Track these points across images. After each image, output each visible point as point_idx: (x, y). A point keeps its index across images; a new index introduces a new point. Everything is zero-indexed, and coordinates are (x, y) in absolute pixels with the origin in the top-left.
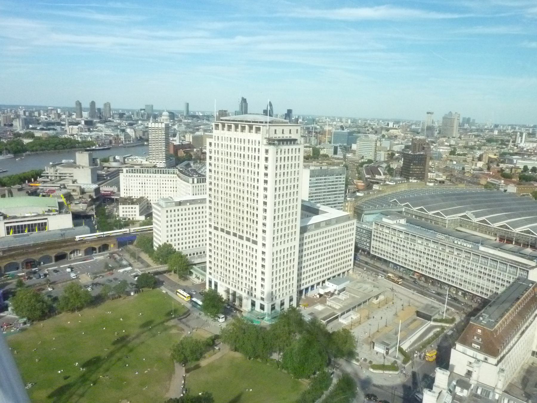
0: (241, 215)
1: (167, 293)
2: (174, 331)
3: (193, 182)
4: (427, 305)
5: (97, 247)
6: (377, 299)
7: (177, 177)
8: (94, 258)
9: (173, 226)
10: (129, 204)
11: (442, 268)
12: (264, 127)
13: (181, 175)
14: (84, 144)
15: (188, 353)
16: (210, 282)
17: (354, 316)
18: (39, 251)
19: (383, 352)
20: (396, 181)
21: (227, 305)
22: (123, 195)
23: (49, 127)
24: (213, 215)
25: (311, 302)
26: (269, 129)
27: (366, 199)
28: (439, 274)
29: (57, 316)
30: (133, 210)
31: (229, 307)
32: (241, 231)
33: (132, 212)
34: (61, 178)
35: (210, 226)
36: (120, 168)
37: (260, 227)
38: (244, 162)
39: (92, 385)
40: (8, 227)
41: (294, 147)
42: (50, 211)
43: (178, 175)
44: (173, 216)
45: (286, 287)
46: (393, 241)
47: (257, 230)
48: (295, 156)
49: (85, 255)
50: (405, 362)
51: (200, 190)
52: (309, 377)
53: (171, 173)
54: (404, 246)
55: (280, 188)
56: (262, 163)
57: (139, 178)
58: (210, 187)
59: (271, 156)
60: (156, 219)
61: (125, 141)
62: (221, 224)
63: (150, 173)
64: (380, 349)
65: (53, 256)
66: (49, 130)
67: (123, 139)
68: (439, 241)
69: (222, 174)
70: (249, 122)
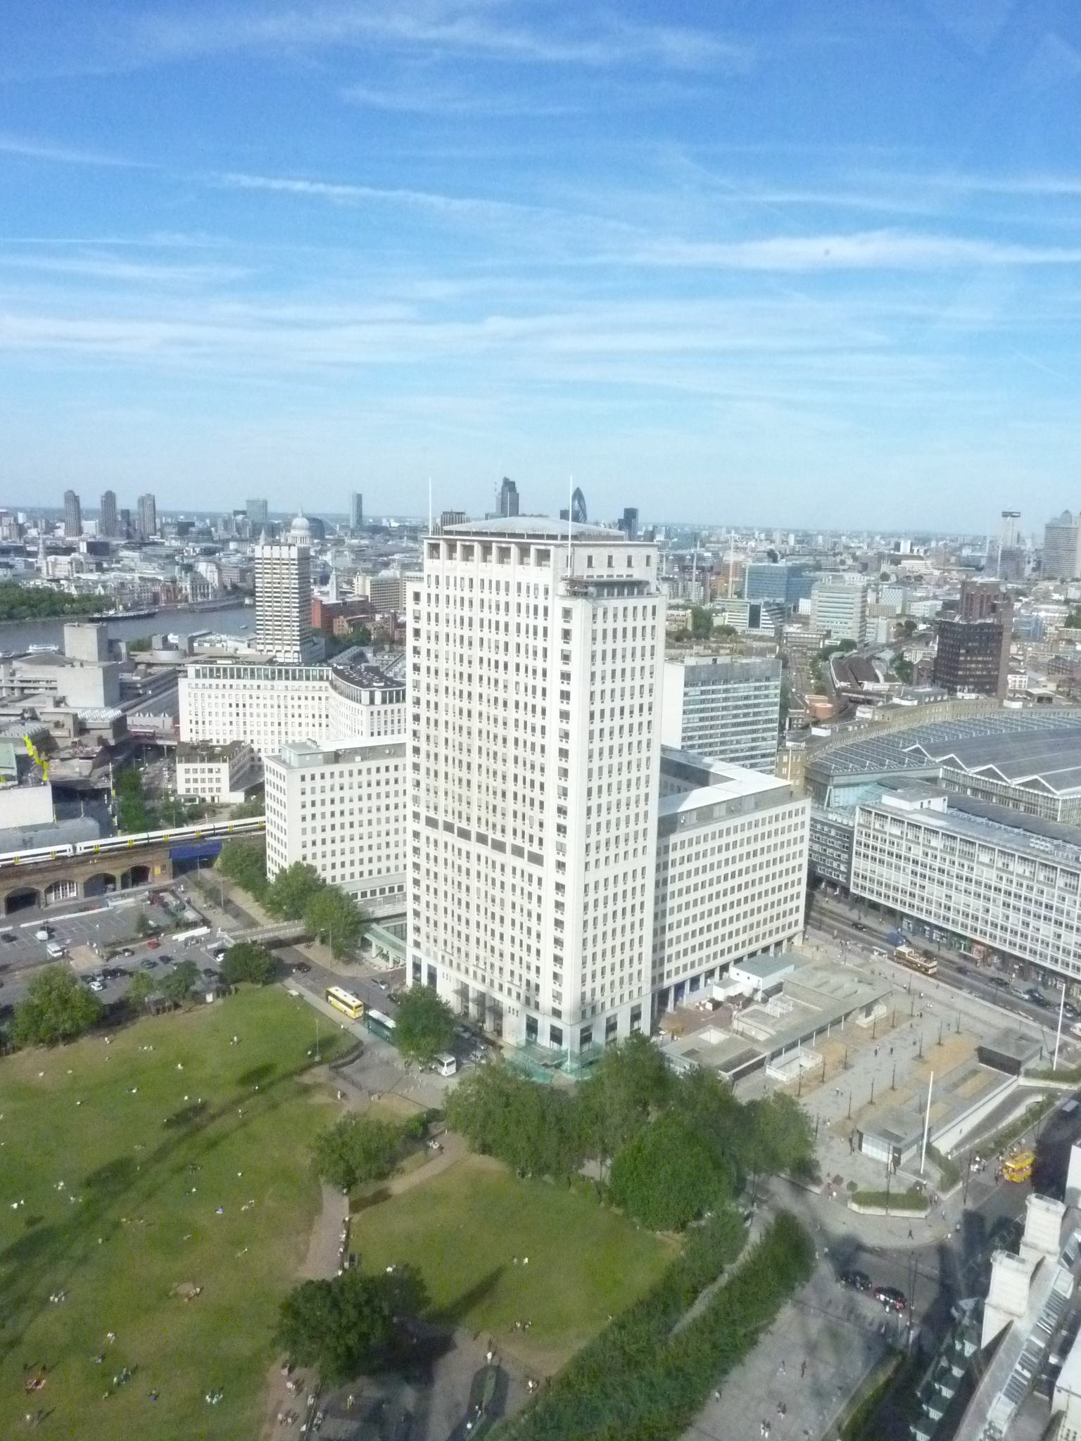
0: (498, 784)
1: (301, 996)
2: (319, 1099)
3: (372, 702)
4: (1008, 1032)
5: (117, 874)
6: (868, 1015)
8: (110, 903)
9: (318, 817)
10: (202, 760)
11: (1047, 930)
12: (560, 549)
13: (340, 682)
14: (88, 605)
15: (356, 1157)
16: (417, 968)
17: (806, 1060)
19: (885, 1160)
20: (919, 697)
21: (461, 1029)
22: (185, 737)
24: (423, 786)
25: (691, 1022)
26: (573, 553)
27: (839, 746)
28: (1039, 948)
29: (12, 1057)
30: (214, 775)
31: (466, 1035)
32: (499, 828)
33: (211, 780)
34: (25, 690)
35: (416, 816)
36: (180, 665)
37: (551, 819)
38: (506, 644)
39: (100, 1241)
41: (639, 602)
43: (331, 683)
44: (318, 790)
45: (622, 979)
46: (911, 856)
47: (541, 825)
48: (644, 628)
50: (946, 1185)
51: (389, 722)
52: (682, 1226)
53: (314, 679)
54: (941, 871)
55: (602, 712)
56: (555, 644)
58: (416, 711)
59: (578, 625)
60: (273, 798)
61: (195, 595)
62: (446, 811)
63: (259, 677)
64: (876, 1151)
67: (189, 591)
68: (1036, 856)
69: (447, 675)
70: (521, 536)
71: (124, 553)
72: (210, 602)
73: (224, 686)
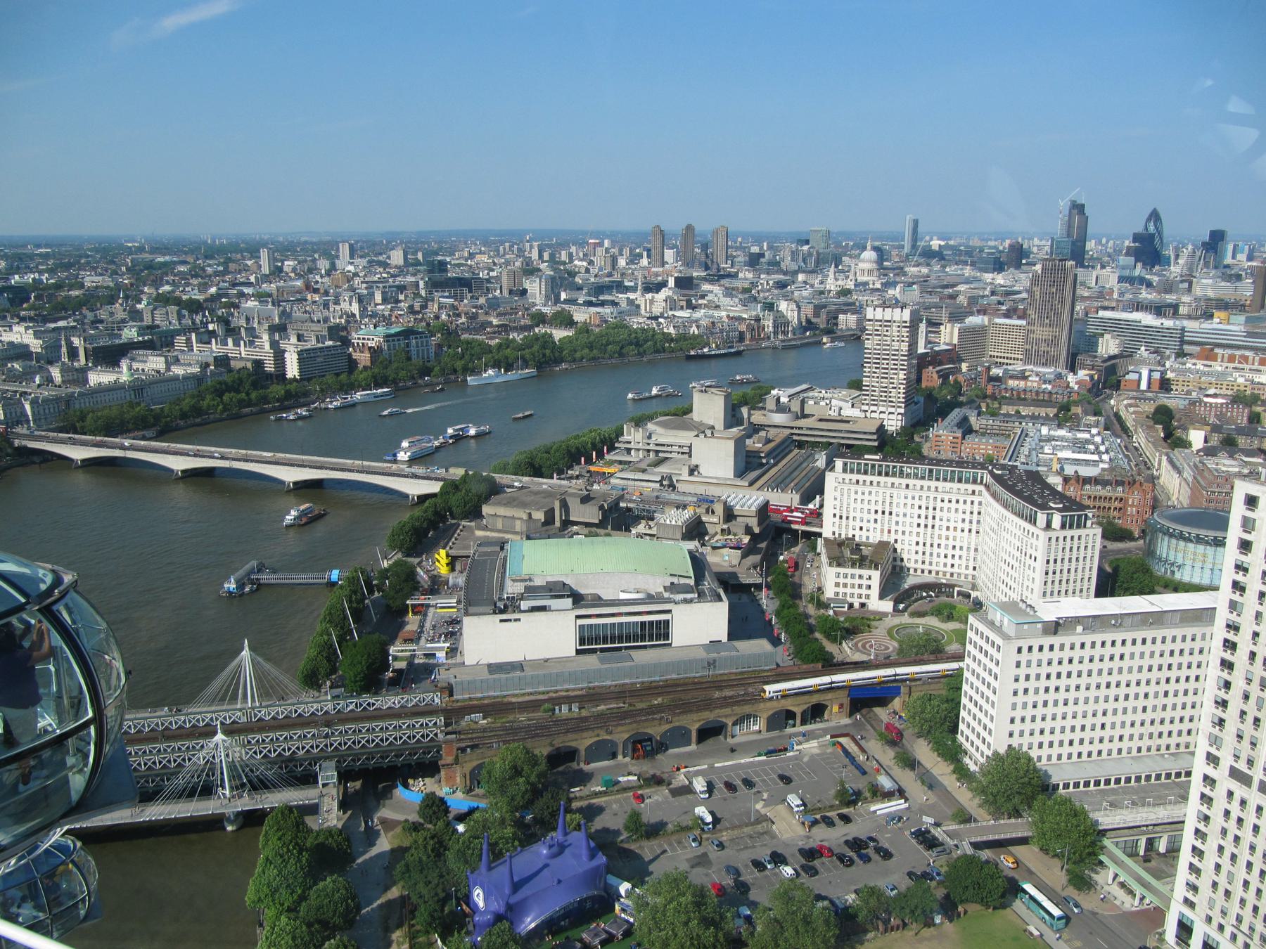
3: (1049, 526)
5: (798, 710)
7: (985, 492)
8: (796, 747)
9: (1031, 692)
10: (853, 566)
13: (998, 488)
14: (684, 344)
18: (660, 708)
23: (601, 298)
36: (792, 428)
40: (583, 626)
42: (672, 588)
43: (987, 487)
44: (1034, 664)
49: (768, 731)
51: (1067, 550)
53: (967, 481)
57: (878, 489)
61: (775, 333)
65: (694, 728)
66: (603, 304)
71: (706, 287)
72: (790, 340)
73: (871, 482)
